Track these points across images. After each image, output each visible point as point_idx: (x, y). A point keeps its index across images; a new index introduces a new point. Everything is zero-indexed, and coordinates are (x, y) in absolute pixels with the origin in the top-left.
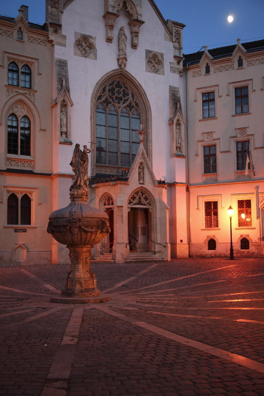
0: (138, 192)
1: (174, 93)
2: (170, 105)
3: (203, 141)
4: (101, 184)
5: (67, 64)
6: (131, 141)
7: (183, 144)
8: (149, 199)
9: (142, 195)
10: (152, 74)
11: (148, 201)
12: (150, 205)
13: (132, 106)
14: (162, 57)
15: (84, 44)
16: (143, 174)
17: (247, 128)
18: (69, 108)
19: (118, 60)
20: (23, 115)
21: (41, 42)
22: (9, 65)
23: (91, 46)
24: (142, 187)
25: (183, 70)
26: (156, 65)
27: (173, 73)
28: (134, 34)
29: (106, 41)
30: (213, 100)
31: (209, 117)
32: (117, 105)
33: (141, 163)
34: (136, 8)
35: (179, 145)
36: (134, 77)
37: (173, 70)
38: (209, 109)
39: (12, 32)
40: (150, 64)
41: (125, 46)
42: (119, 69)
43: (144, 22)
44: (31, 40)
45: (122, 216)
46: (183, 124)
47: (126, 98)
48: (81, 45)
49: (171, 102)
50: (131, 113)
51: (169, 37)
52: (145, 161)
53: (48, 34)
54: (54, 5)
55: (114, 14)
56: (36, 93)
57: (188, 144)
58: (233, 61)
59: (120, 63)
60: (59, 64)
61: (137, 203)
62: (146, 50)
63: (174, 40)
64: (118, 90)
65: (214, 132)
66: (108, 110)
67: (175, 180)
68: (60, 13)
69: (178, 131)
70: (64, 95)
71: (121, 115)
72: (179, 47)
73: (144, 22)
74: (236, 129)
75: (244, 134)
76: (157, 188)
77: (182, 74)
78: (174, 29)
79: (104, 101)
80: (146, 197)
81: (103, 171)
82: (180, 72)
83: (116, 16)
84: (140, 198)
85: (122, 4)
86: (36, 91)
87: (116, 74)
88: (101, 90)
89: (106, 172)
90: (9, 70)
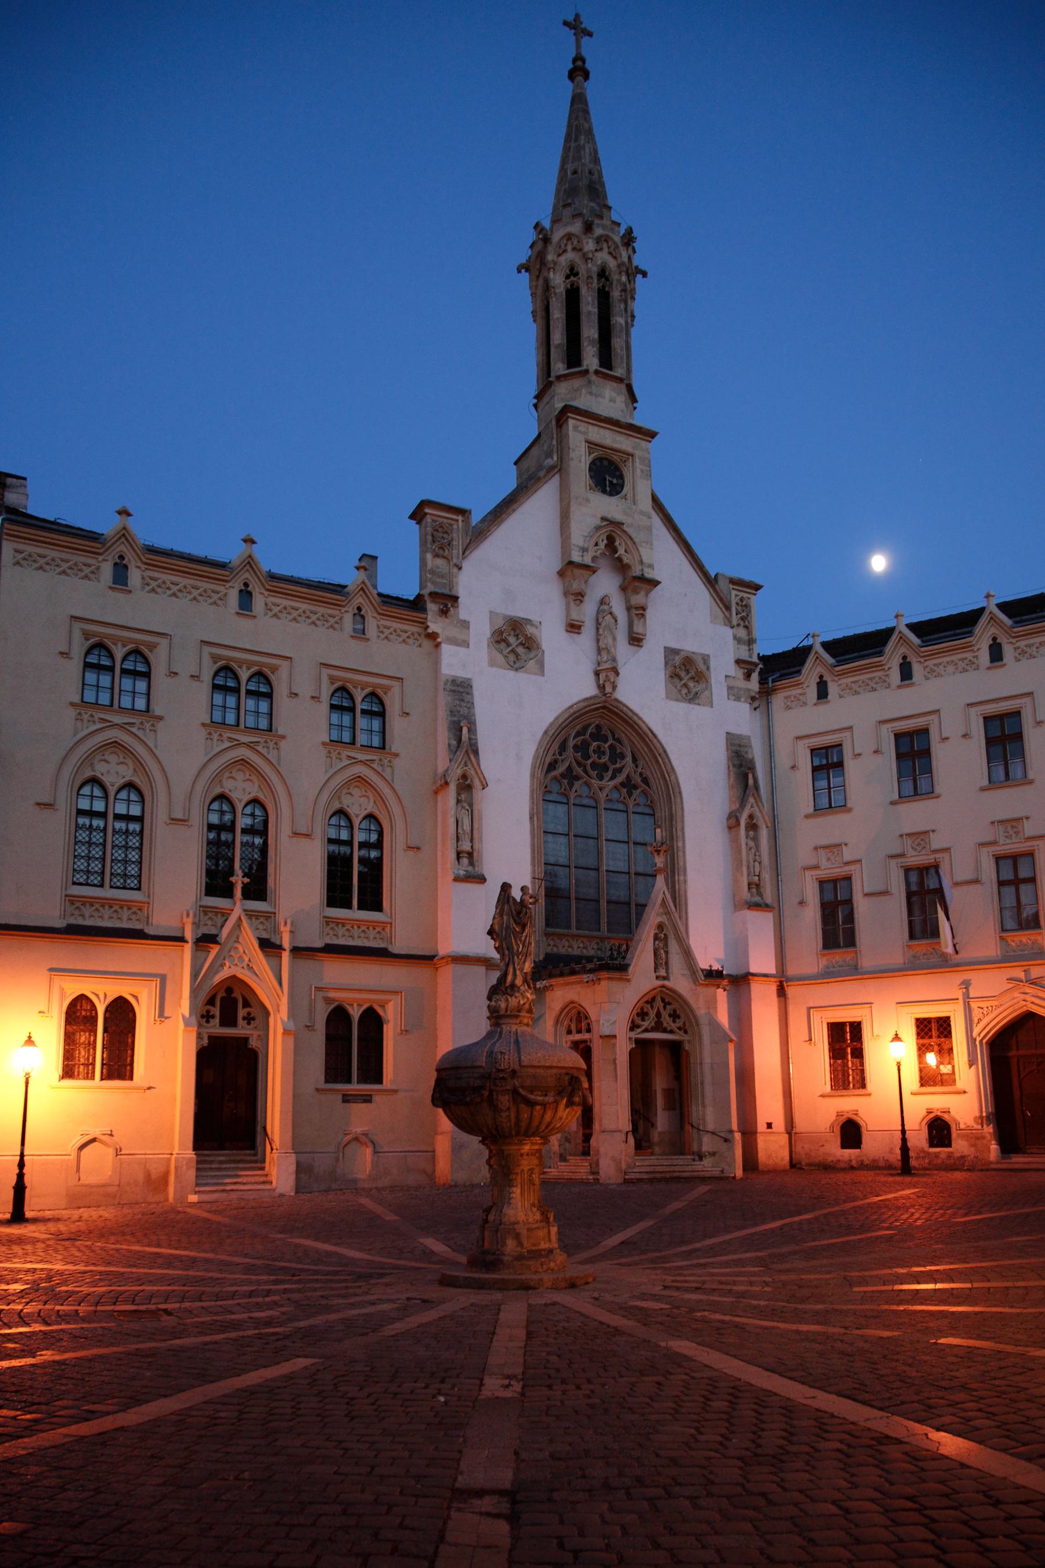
0: (653, 999)
2: (729, 779)
3: (816, 867)
4: (560, 980)
5: (471, 687)
6: (632, 872)
7: (767, 876)
8: (682, 1016)
9: (665, 1008)
10: (682, 707)
11: (679, 1023)
12: (686, 1032)
13: (576, 776)
14: (705, 663)
15: (512, 640)
16: (667, 953)
17: (931, 833)
18: (478, 793)
19: (597, 674)
20: (364, 813)
21: (408, 637)
22: (332, 695)
23: (530, 644)
24: (663, 986)
25: (759, 692)
26: (691, 684)
28: (634, 611)
29: (568, 631)
30: (840, 764)
31: (830, 807)
32: (595, 783)
33: (660, 927)
34: (638, 549)
35: (757, 878)
36: (637, 715)
38: (829, 788)
39: (98, 568)
40: (676, 680)
41: (614, 639)
42: (600, 695)
43: (657, 583)
44: (329, 624)
45: (615, 1060)
46: (764, 827)
47: (618, 765)
48: (505, 641)
49: (732, 773)
50: (631, 803)
51: (722, 615)
52: (670, 919)
53: (426, 619)
54: (441, 552)
55: (586, 567)
56: (398, 759)
57: (778, 876)
58: (886, 667)
59: (601, 682)
60: (453, 688)
61: (652, 1028)
62: (665, 648)
63: (735, 622)
64: (599, 747)
65: (846, 844)
66: (572, 795)
67: (748, 967)
68: (455, 570)
69: (752, 844)
70: (466, 763)
71: (607, 807)
72: (746, 638)
73: (657, 583)
74: (901, 836)
75: (924, 848)
76: (700, 989)
77: (756, 704)
78: (733, 596)
79: (562, 775)
80: (675, 1011)
81: (563, 948)
82: (753, 699)
83: (591, 569)
84: (658, 1015)
85: (605, 541)
86: (397, 755)
87: (593, 707)
88: (556, 746)
89: (570, 950)
90: (333, 707)
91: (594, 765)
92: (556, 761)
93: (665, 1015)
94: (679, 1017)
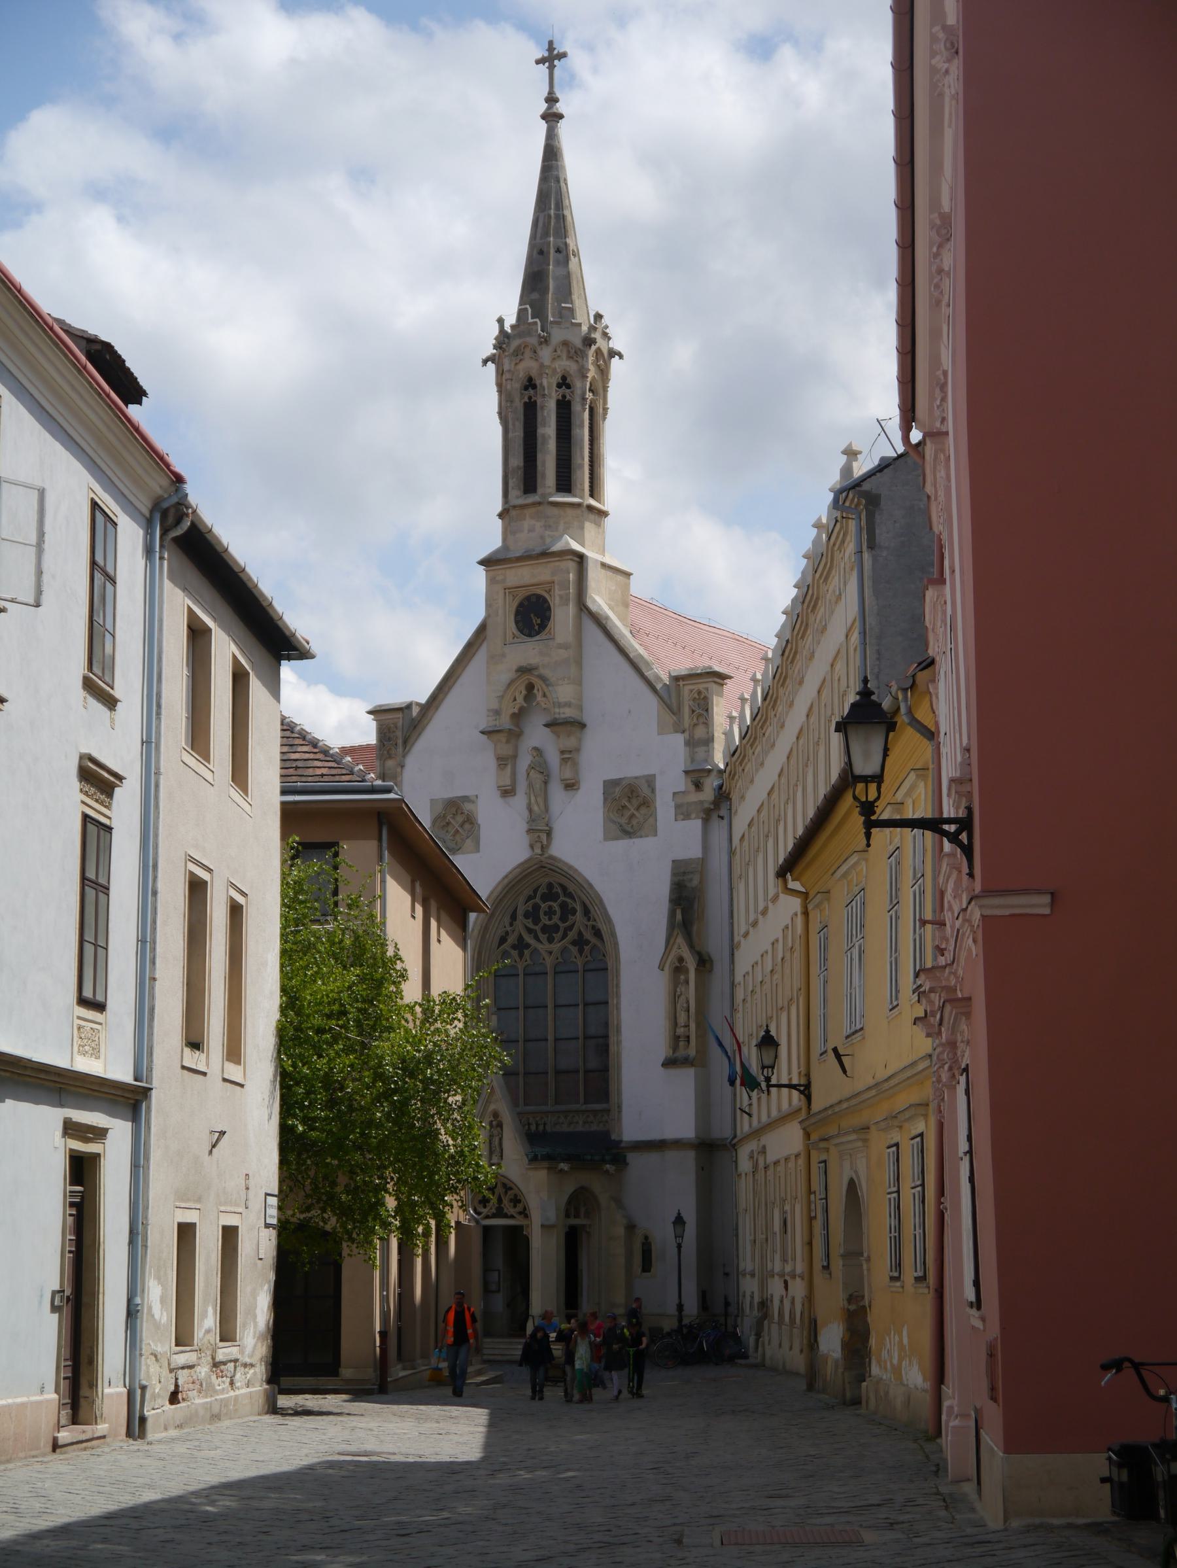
1: (683, 880)
9: (506, 1193)
11: (520, 1208)
16: (501, 1139)
27: (683, 820)
37: (682, 814)
80: (516, 1195)
84: (500, 1200)
91: (545, 929)
92: (507, 933)
93: (505, 1201)
94: (519, 1201)
